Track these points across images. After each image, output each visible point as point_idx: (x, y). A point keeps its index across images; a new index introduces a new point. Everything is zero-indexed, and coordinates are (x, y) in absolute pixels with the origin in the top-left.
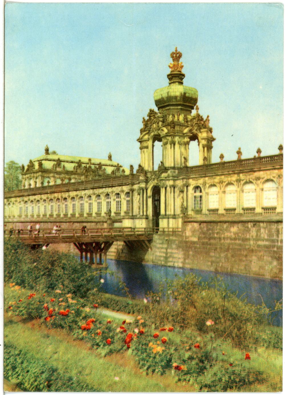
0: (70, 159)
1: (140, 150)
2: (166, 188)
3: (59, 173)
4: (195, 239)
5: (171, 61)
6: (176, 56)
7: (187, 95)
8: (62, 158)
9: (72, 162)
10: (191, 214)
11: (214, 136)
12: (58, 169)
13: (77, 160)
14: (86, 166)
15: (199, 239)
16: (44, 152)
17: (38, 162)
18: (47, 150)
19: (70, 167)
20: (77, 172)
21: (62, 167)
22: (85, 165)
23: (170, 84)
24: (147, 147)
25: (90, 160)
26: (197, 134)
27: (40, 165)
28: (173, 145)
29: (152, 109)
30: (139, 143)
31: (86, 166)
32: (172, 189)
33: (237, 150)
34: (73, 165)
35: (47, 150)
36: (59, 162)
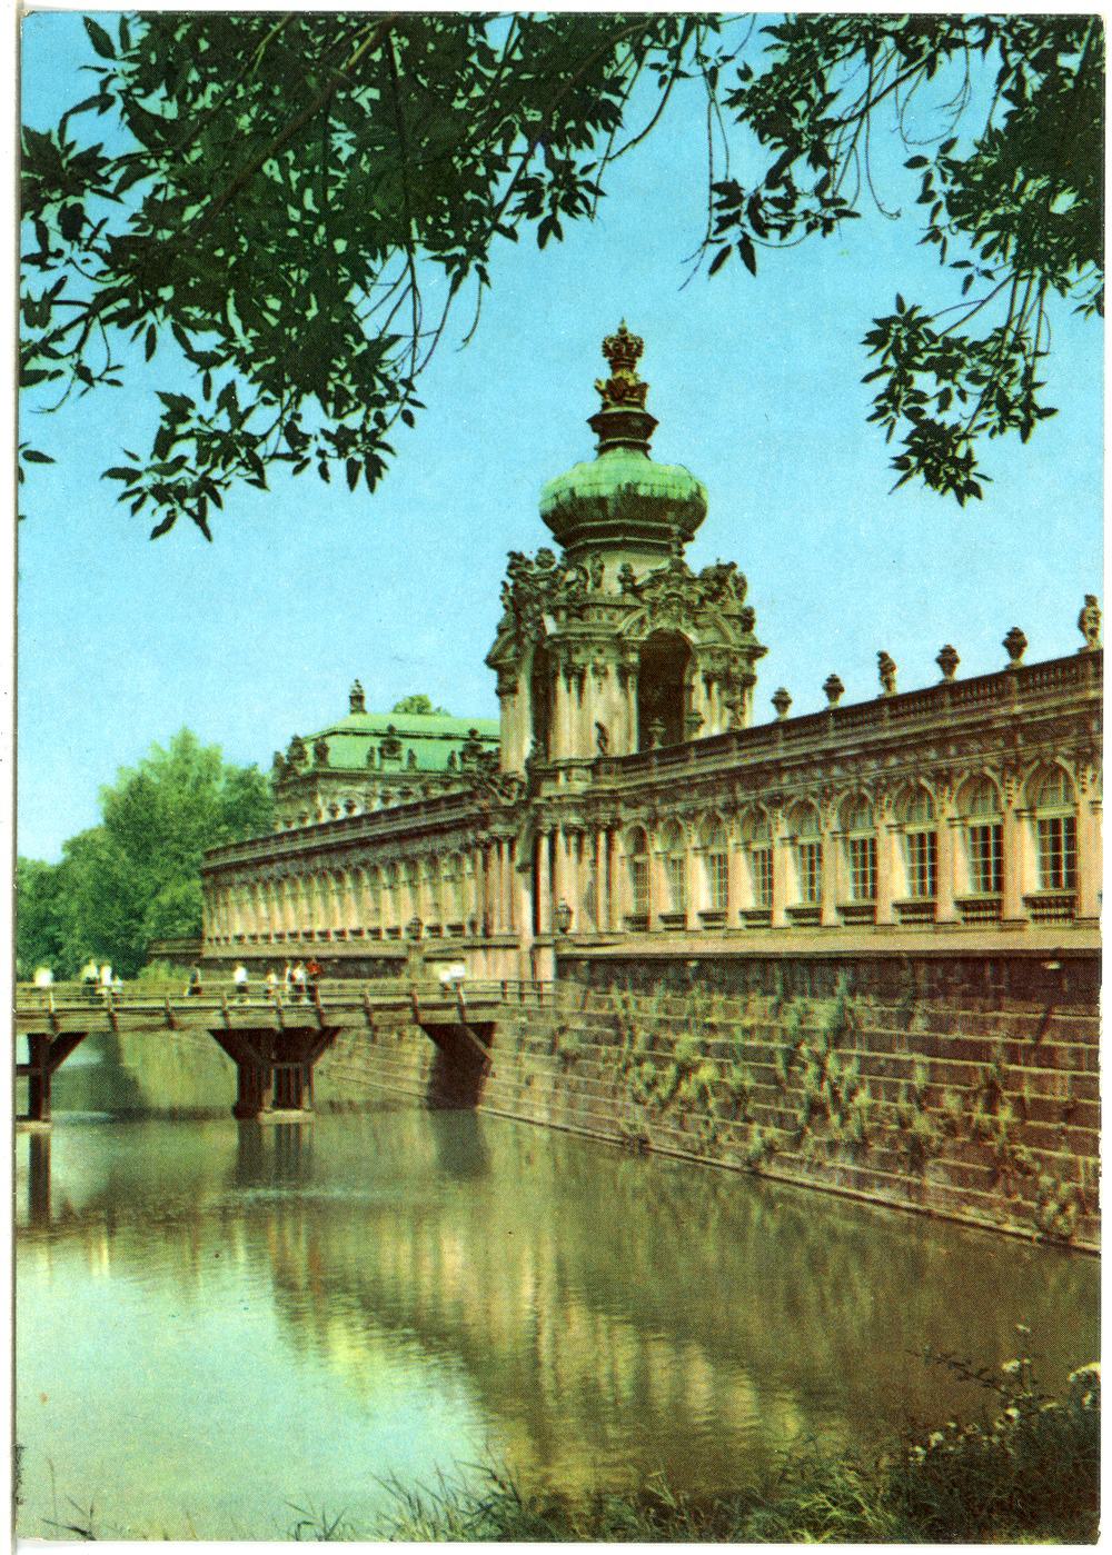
1: (496, 700)
6: (622, 351)
9: (447, 737)
11: (762, 643)
12: (391, 768)
13: (464, 732)
18: (357, 699)
19: (434, 757)
23: (602, 450)
26: (678, 631)
27: (322, 752)
28: (573, 681)
30: (494, 673)
32: (573, 840)
35: (357, 699)
36: (390, 742)
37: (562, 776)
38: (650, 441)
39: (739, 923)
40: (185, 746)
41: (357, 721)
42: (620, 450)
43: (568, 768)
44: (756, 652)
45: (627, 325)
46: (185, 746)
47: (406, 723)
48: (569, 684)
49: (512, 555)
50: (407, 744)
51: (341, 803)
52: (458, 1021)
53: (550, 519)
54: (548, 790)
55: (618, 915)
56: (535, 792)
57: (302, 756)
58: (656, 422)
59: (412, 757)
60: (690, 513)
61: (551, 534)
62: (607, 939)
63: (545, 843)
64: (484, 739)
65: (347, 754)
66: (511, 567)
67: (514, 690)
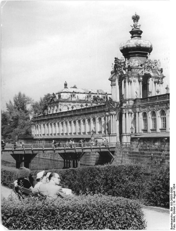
0: (82, 91)
2: (125, 114)
3: (74, 102)
4: (137, 151)
5: (132, 23)
6: (136, 18)
7: (142, 46)
10: (141, 132)
11: (164, 75)
14: (95, 96)
15: (139, 151)
16: (64, 86)
17: (58, 95)
18: (66, 85)
19: (82, 97)
20: (88, 100)
22: (94, 95)
23: (132, 37)
24: (115, 85)
25: (98, 91)
26: (149, 73)
27: (60, 96)
28: (130, 83)
29: (117, 57)
30: (111, 81)
31: (95, 96)
32: (130, 114)
33: (166, 86)
34: (85, 95)
35: (66, 85)
36: (73, 94)
37: (127, 102)
38: (141, 35)
39: (159, 131)
40: (20, 94)
41: (65, 90)
42: (136, 37)
43: (129, 100)
44: (163, 77)
45: (136, 13)
46: (20, 94)
47: (75, 90)
48: (129, 84)
49: (115, 58)
50: (77, 95)
51: (70, 107)
52: (75, 152)
53: (122, 51)
54: (124, 105)
56: (121, 105)
57: (55, 97)
58: (142, 32)
60: (149, 50)
61: (122, 54)
62: (138, 134)
63: (124, 115)
64: (93, 94)
65: (64, 96)
66: (115, 61)
67: (115, 85)
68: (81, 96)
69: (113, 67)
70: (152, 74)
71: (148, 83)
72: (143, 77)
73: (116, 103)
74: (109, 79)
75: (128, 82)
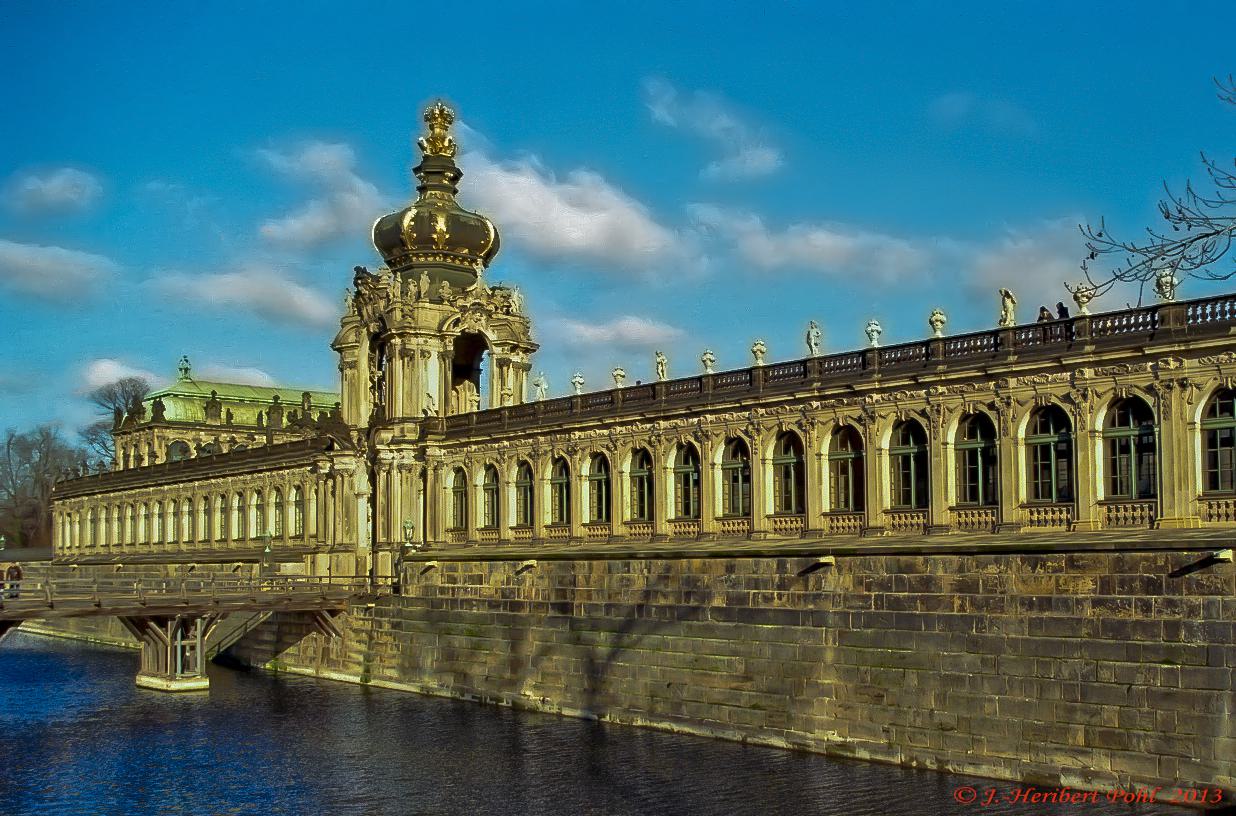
2: (389, 473)
8: (221, 393)
21: (223, 415)
27: (159, 407)
36: (212, 405)
43: (404, 420)
49: (358, 269)
55: (441, 529)
59: (230, 416)
63: (383, 475)
66: (357, 279)
67: (354, 365)
68: (242, 410)
69: (350, 302)
70: (491, 336)
71: (475, 367)
72: (457, 341)
73: (360, 431)
74: (332, 346)
75: (402, 358)
